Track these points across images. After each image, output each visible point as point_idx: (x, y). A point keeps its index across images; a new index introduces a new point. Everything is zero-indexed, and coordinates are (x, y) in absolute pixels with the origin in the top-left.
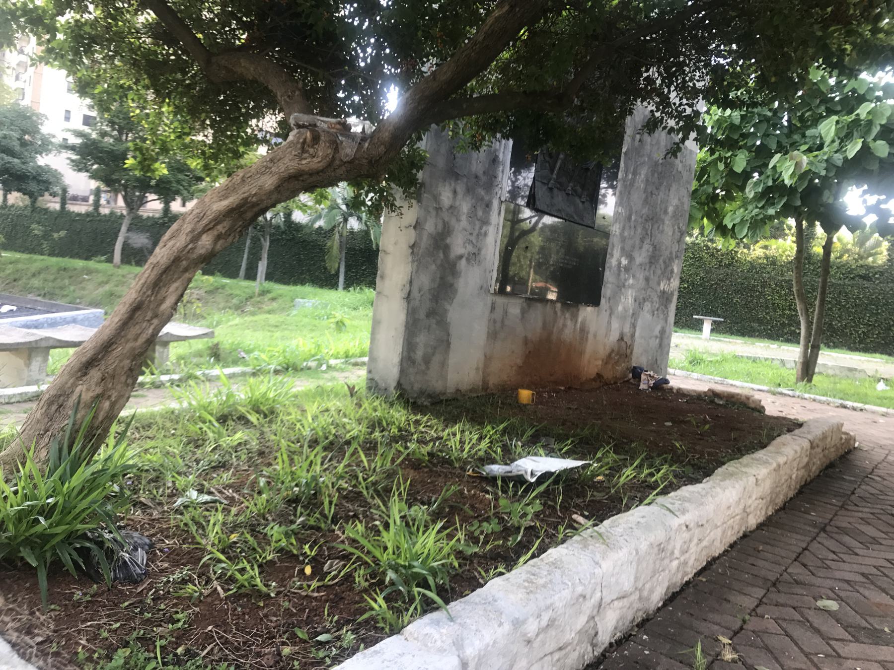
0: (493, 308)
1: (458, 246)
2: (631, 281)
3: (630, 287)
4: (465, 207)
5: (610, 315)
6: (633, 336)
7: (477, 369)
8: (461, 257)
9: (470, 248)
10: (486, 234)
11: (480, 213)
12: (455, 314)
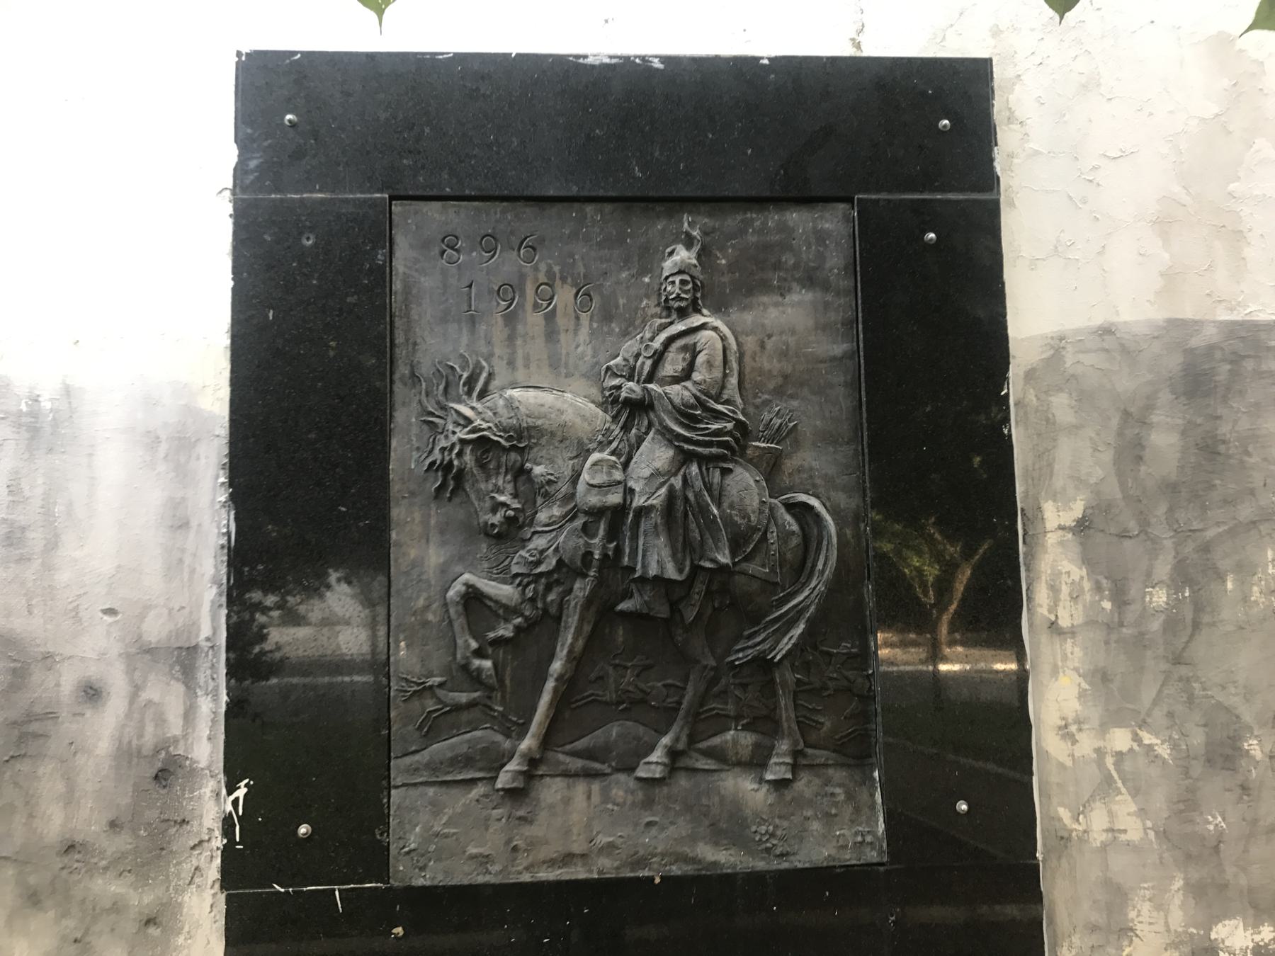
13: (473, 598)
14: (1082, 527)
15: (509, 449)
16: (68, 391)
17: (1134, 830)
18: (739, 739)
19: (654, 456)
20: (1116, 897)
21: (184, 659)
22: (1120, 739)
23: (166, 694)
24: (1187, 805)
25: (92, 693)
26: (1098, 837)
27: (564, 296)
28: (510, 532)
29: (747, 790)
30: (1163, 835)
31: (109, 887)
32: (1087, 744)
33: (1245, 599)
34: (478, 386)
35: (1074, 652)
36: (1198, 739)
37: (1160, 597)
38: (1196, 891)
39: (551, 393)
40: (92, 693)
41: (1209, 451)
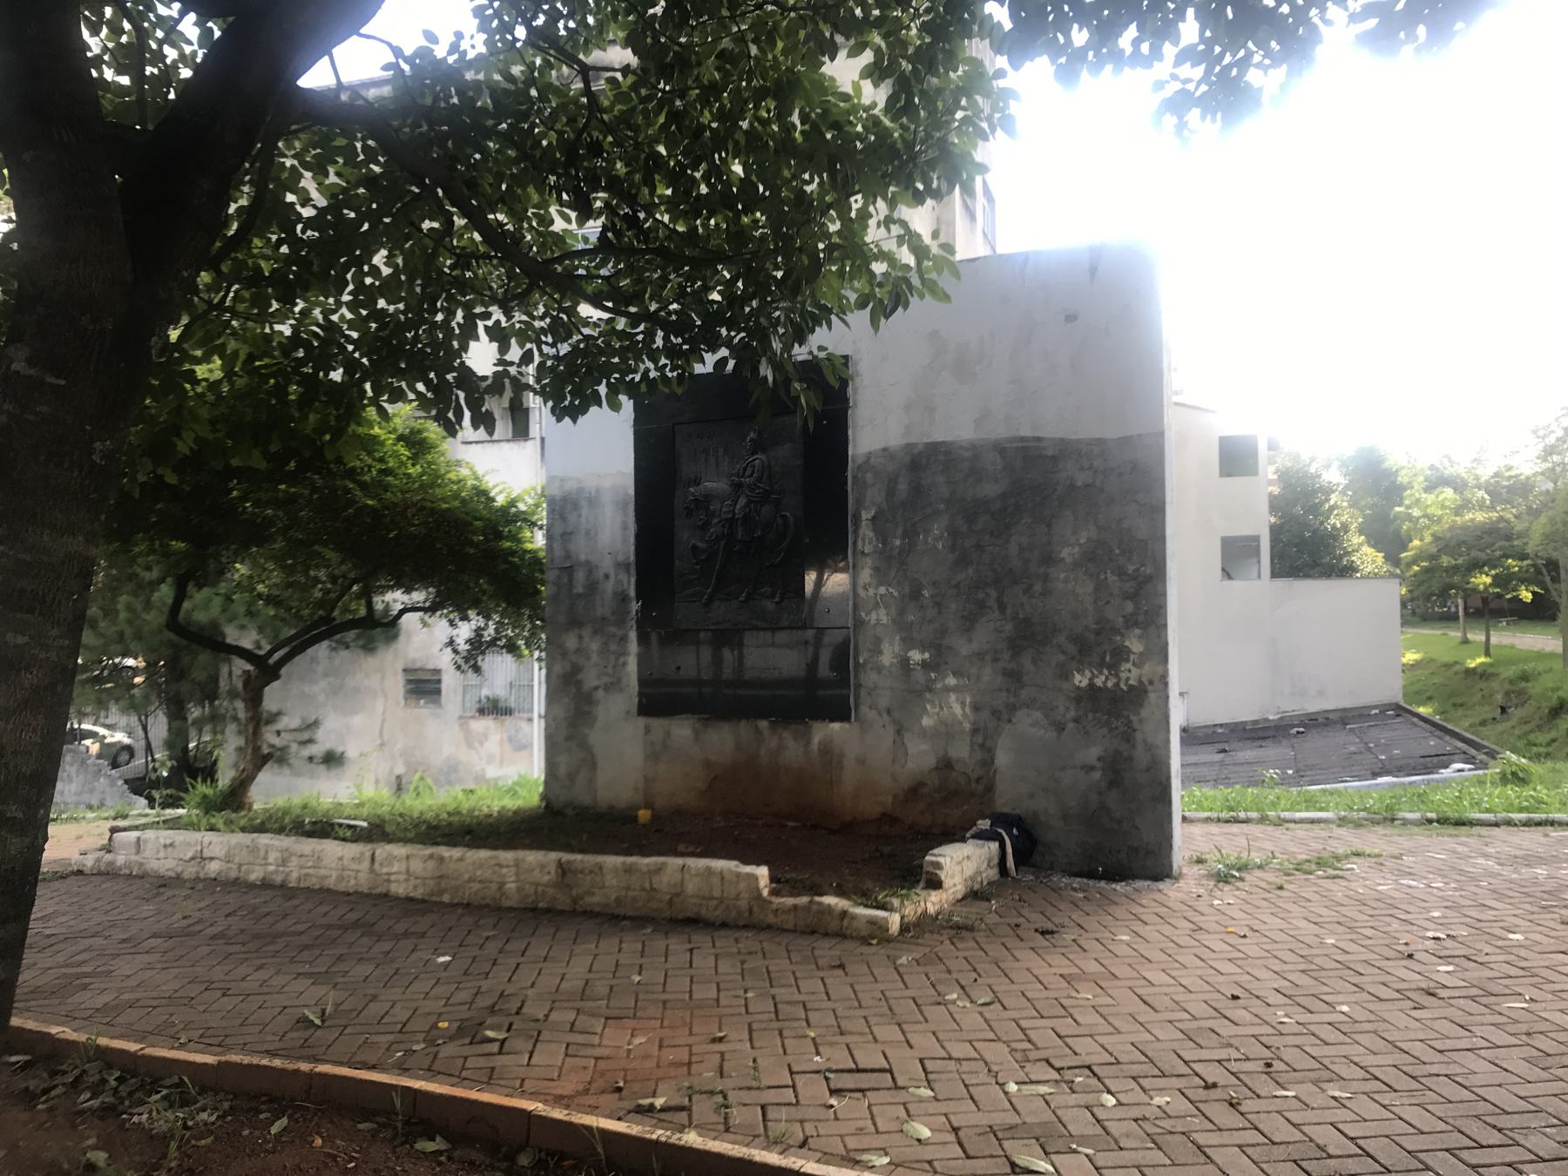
0: (648, 730)
1: (590, 679)
2: (951, 681)
3: (948, 689)
4: (595, 646)
5: (899, 732)
6: (988, 762)
7: (636, 789)
8: (597, 688)
9: (606, 679)
10: (625, 664)
11: (613, 647)
12: (596, 738)
13: (694, 547)
14: (874, 519)
15: (703, 502)
16: (598, 491)
17: (884, 619)
18: (767, 590)
19: (742, 501)
20: (878, 641)
21: (627, 566)
22: (882, 590)
23: (623, 577)
24: (902, 612)
25: (607, 576)
26: (873, 622)
27: (721, 450)
28: (705, 526)
29: (770, 605)
30: (894, 621)
31: (613, 629)
32: (871, 592)
33: (926, 542)
34: (697, 482)
35: (869, 561)
36: (907, 590)
37: (898, 542)
38: (903, 640)
39: (715, 485)
40: (607, 576)
41: (917, 490)
